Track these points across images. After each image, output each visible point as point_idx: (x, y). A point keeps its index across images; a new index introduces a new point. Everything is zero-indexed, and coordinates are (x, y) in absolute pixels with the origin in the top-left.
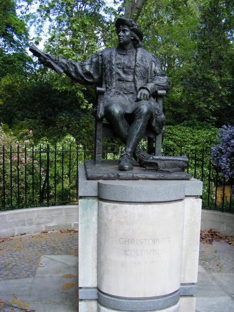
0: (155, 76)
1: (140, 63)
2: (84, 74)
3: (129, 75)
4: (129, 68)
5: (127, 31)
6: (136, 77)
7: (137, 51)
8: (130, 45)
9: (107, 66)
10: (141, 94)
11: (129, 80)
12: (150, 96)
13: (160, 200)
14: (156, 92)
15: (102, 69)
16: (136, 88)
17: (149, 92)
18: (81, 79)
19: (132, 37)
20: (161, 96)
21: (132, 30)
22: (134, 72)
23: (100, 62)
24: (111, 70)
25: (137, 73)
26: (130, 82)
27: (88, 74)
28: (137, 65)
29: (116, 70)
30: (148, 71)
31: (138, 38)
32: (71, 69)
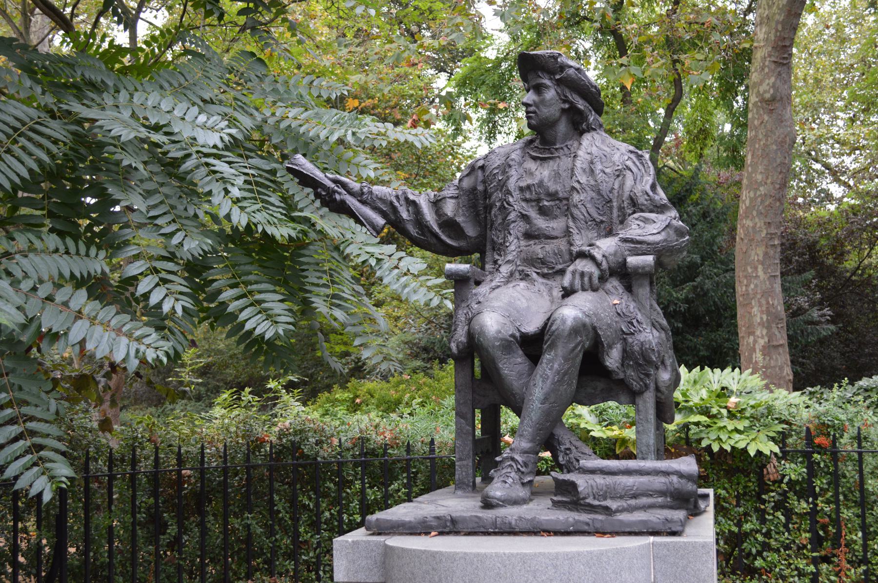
1: (583, 179)
2: (440, 226)
3: (555, 217)
4: (553, 196)
5: (547, 87)
8: (562, 127)
10: (574, 273)
11: (554, 233)
12: (602, 279)
17: (598, 265)
18: (433, 241)
19: (565, 101)
21: (559, 82)
23: (480, 188)
25: (575, 212)
26: (556, 238)
27: (449, 225)
30: (610, 201)
31: (581, 104)
32: (405, 215)
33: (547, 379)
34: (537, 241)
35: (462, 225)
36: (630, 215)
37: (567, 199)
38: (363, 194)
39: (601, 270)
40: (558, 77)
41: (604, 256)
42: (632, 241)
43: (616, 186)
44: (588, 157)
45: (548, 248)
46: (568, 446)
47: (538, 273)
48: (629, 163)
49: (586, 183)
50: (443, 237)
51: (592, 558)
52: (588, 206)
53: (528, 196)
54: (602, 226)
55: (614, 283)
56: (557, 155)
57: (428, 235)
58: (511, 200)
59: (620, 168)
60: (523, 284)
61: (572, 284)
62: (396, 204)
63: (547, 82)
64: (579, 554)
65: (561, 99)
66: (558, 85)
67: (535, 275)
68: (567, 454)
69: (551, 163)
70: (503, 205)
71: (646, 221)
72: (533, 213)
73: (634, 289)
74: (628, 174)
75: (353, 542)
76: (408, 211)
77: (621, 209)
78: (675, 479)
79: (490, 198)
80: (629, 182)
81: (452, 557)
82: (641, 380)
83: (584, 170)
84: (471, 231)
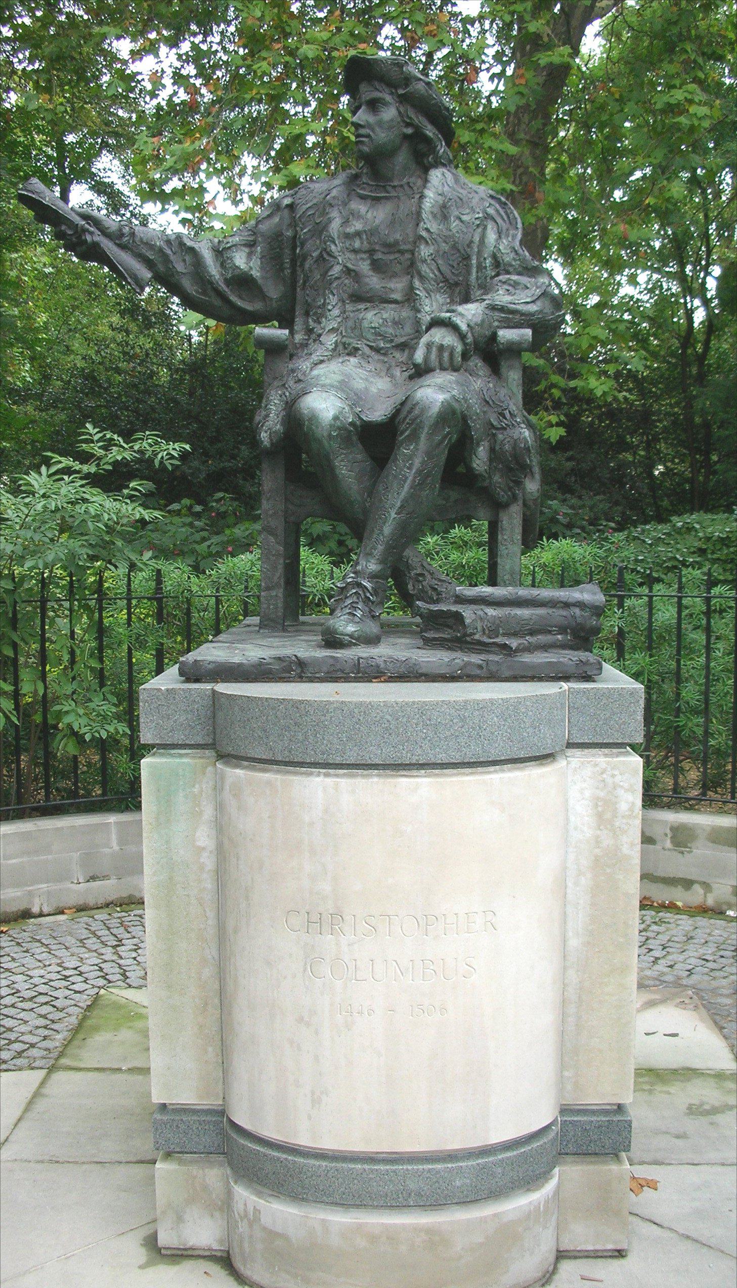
1: (434, 227)
2: (228, 282)
3: (394, 275)
4: (391, 247)
5: (386, 104)
6: (417, 283)
7: (426, 181)
8: (402, 157)
9: (308, 245)
10: (429, 346)
12: (465, 356)
13: (442, 758)
14: (494, 336)
15: (293, 262)
16: (418, 322)
17: (462, 337)
18: (217, 302)
19: (408, 125)
20: (514, 350)
21: (404, 99)
22: (412, 264)
23: (289, 233)
24: (325, 258)
25: (424, 269)
26: (395, 302)
27: (243, 282)
28: (424, 234)
29: (342, 259)
31: (430, 131)
32: (180, 267)
33: (405, 481)
34: (368, 305)
35: (260, 281)
36: (492, 278)
38: (123, 235)
39: (465, 344)
40: (401, 92)
41: (468, 326)
42: (502, 309)
43: (477, 239)
44: (440, 200)
46: (419, 571)
47: (371, 347)
48: (491, 211)
49: (437, 232)
50: (233, 298)
51: (507, 708)
52: (440, 262)
53: (357, 244)
55: (476, 362)
56: (394, 194)
57: (212, 294)
58: (333, 247)
59: (481, 215)
60: (353, 360)
61: (426, 359)
62: (169, 252)
63: (388, 98)
64: (492, 701)
65: (404, 121)
66: (401, 102)
67: (367, 350)
68: (419, 581)
71: (515, 285)
73: (503, 370)
74: (490, 225)
75: (167, 690)
77: (480, 267)
78: (577, 611)
79: (302, 245)
81: (323, 707)
82: (510, 489)
83: (434, 216)
84: (274, 291)
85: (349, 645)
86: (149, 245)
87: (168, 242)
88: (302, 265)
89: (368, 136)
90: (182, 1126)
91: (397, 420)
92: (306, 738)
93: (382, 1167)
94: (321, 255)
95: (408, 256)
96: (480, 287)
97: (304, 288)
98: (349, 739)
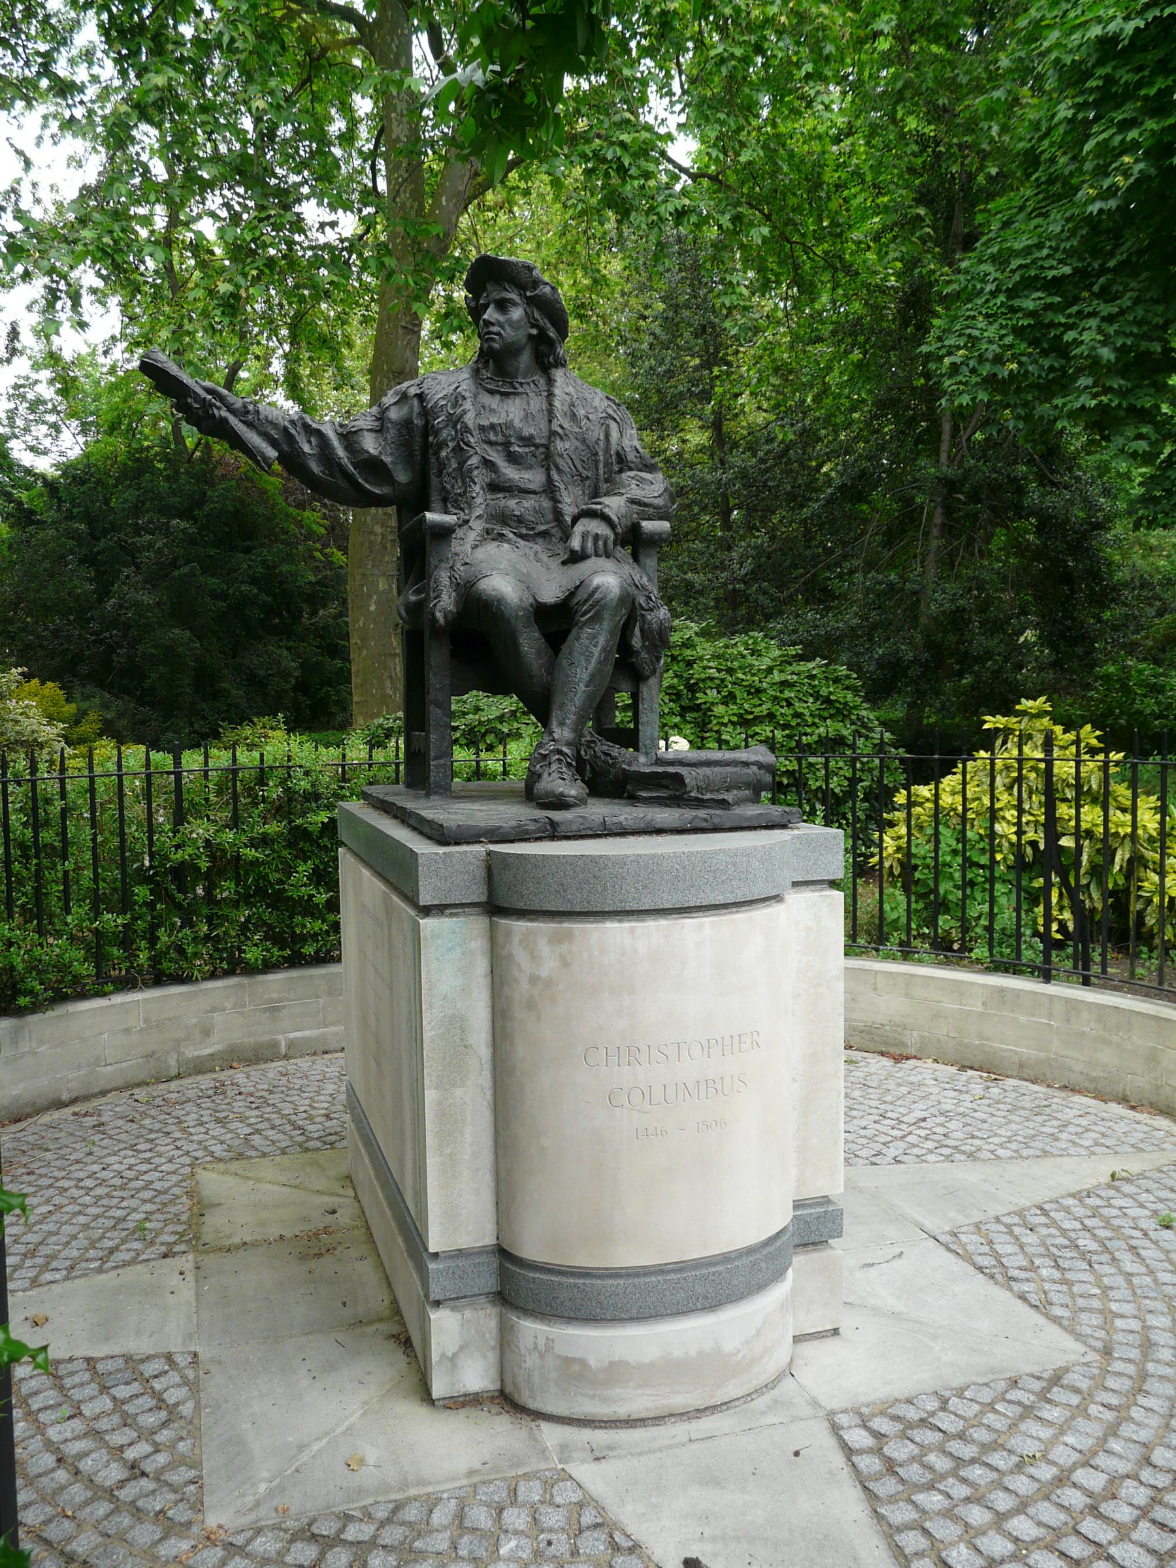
0: (621, 471)
3: (530, 467)
4: (527, 441)
5: (515, 304)
6: (555, 476)
7: (550, 382)
8: (525, 358)
9: (445, 433)
10: (584, 536)
11: (532, 487)
13: (720, 899)
15: (426, 446)
16: (558, 514)
18: (343, 484)
19: (533, 326)
20: (654, 541)
21: (532, 302)
22: (548, 456)
26: (535, 493)
27: (373, 466)
29: (478, 450)
31: (552, 333)
32: (306, 448)
37: (547, 447)
38: (248, 412)
39: (616, 534)
45: (526, 504)
48: (610, 411)
53: (492, 437)
54: (587, 483)
56: (520, 390)
57: (338, 475)
58: (472, 440)
61: (583, 547)
62: (293, 431)
63: (513, 296)
64: (755, 848)
67: (511, 536)
69: (518, 400)
70: (458, 445)
72: (496, 456)
73: (642, 558)
76: (309, 442)
77: (607, 464)
78: (755, 768)
80: (615, 434)
81: (621, 861)
84: (402, 476)
85: (575, 805)
86: (275, 425)
87: (292, 422)
88: (437, 453)
89: (498, 334)
90: (458, 1272)
91: (575, 601)
92: (605, 889)
93: (673, 1276)
94: (458, 445)
95: (542, 450)
96: (607, 481)
97: (440, 474)
98: (645, 887)
